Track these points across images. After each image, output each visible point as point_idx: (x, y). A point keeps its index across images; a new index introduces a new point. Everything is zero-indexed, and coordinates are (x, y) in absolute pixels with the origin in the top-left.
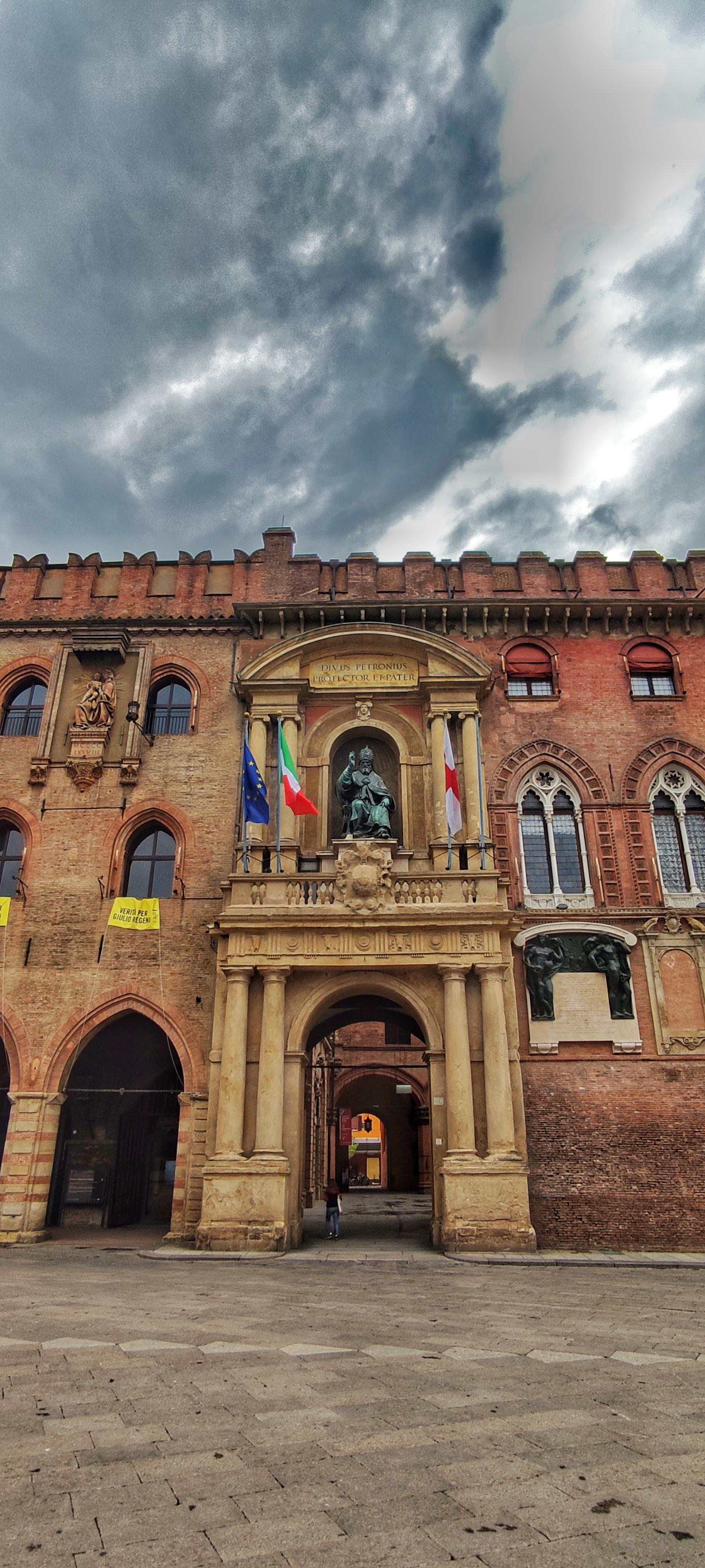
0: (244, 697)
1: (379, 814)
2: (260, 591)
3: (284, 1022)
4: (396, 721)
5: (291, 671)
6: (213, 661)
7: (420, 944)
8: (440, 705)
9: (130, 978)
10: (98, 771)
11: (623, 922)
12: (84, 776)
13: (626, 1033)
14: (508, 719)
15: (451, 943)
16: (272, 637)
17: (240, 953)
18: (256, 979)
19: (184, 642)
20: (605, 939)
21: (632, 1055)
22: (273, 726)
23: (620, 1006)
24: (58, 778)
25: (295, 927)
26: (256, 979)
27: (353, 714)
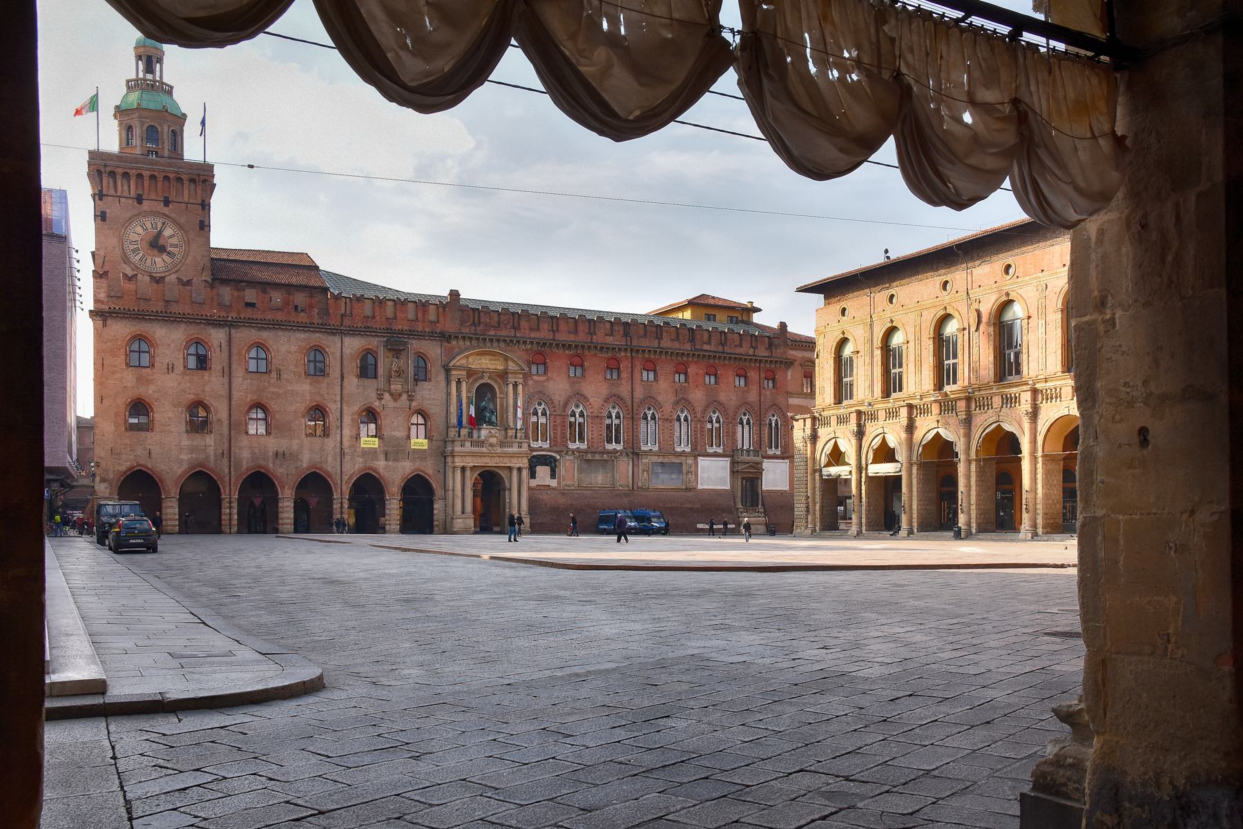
0: (447, 371)
1: (494, 418)
2: (450, 325)
3: (470, 478)
4: (496, 381)
5: (463, 362)
6: (434, 350)
7: (506, 460)
8: (511, 379)
9: (418, 464)
10: (400, 395)
11: (556, 452)
12: (396, 397)
13: (554, 483)
14: (530, 382)
15: (514, 460)
16: (454, 343)
17: (459, 462)
18: (463, 469)
19: (423, 343)
20: (551, 457)
21: (554, 489)
22: (459, 382)
23: (553, 476)
24: (387, 396)
25: (473, 455)
26: (463, 469)
27: (482, 377)
